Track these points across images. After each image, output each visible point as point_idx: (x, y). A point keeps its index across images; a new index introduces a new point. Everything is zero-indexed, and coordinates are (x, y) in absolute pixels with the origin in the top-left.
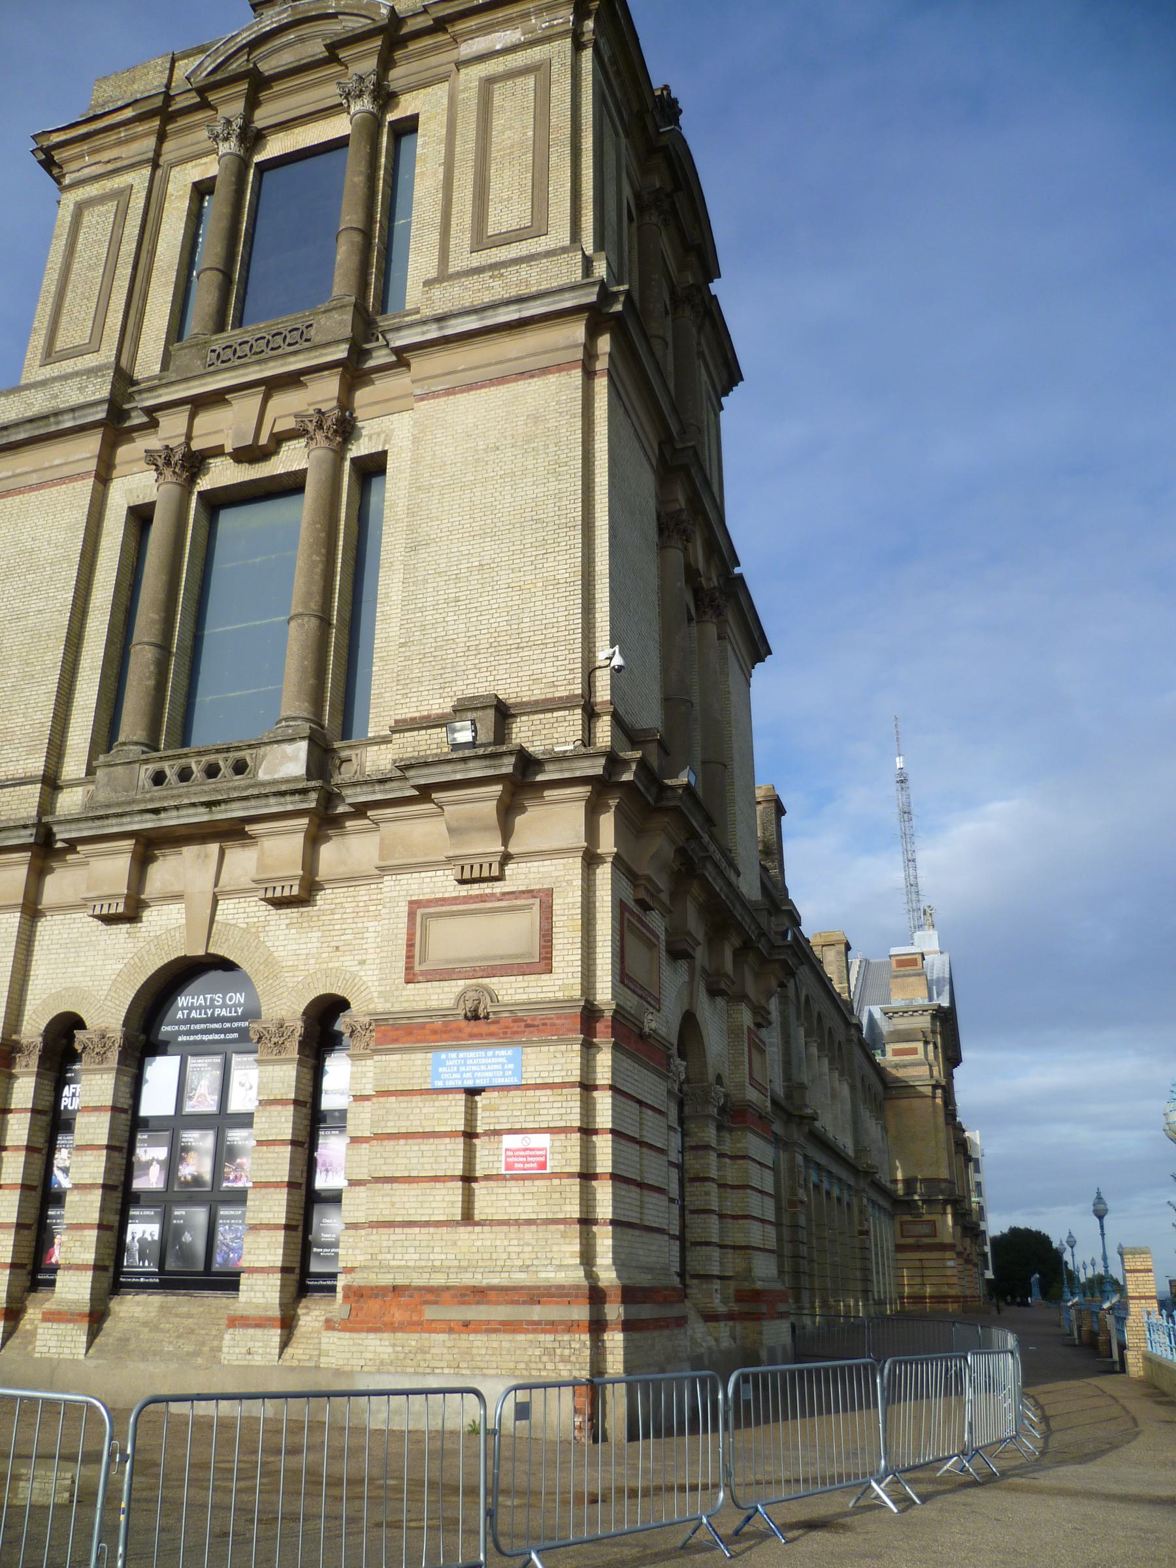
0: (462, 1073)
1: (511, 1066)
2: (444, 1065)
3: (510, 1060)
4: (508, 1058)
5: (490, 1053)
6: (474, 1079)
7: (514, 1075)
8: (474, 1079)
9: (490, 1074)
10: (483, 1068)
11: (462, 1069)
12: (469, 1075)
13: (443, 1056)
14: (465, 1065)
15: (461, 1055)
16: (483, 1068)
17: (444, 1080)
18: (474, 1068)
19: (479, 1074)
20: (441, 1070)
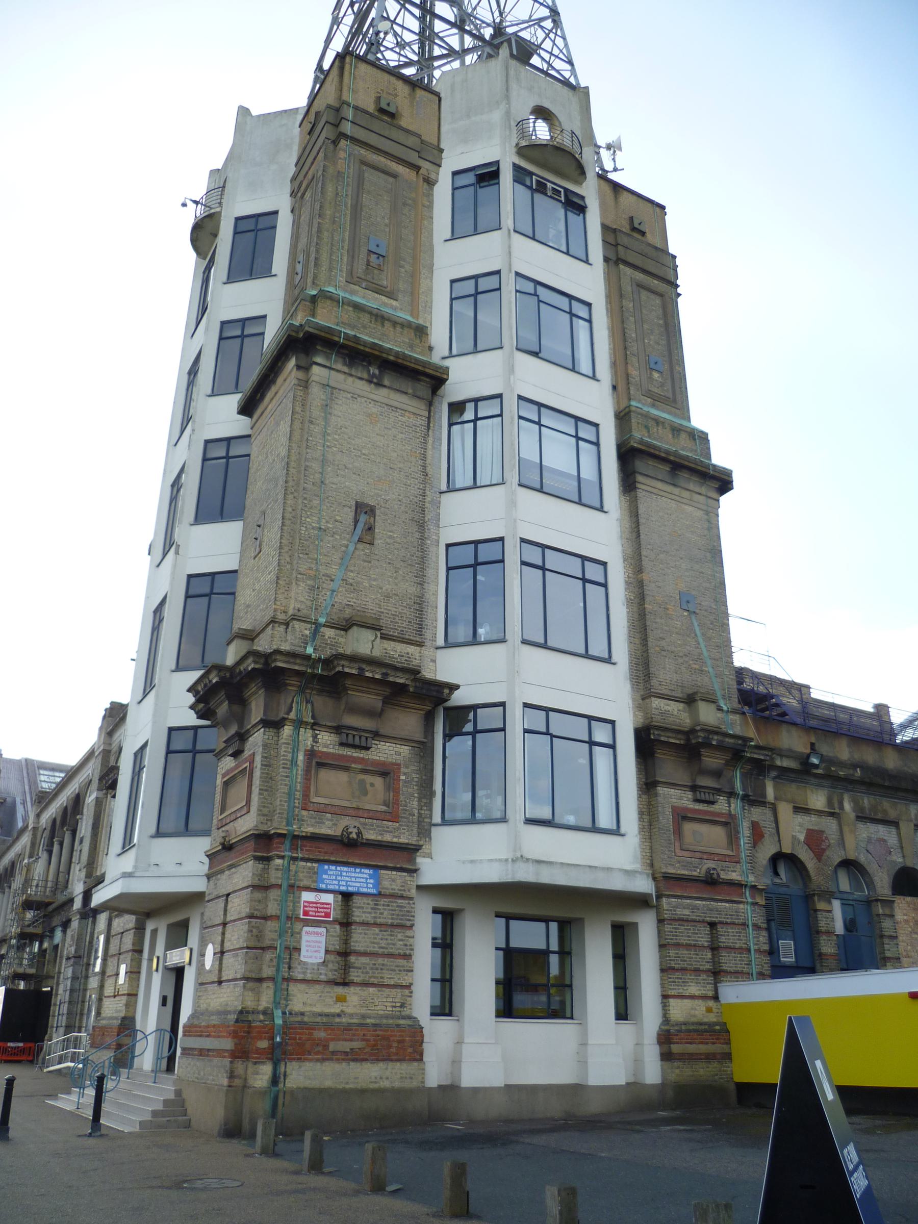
0: (339, 881)
1: (372, 881)
2: (326, 874)
3: (371, 877)
4: (370, 875)
5: (358, 870)
6: (347, 886)
7: (373, 888)
8: (347, 886)
9: (358, 885)
10: (353, 879)
11: (339, 878)
12: (344, 883)
13: (326, 867)
14: (341, 875)
15: (339, 868)
16: (353, 879)
17: (327, 885)
18: (347, 879)
19: (351, 884)
20: (324, 876)
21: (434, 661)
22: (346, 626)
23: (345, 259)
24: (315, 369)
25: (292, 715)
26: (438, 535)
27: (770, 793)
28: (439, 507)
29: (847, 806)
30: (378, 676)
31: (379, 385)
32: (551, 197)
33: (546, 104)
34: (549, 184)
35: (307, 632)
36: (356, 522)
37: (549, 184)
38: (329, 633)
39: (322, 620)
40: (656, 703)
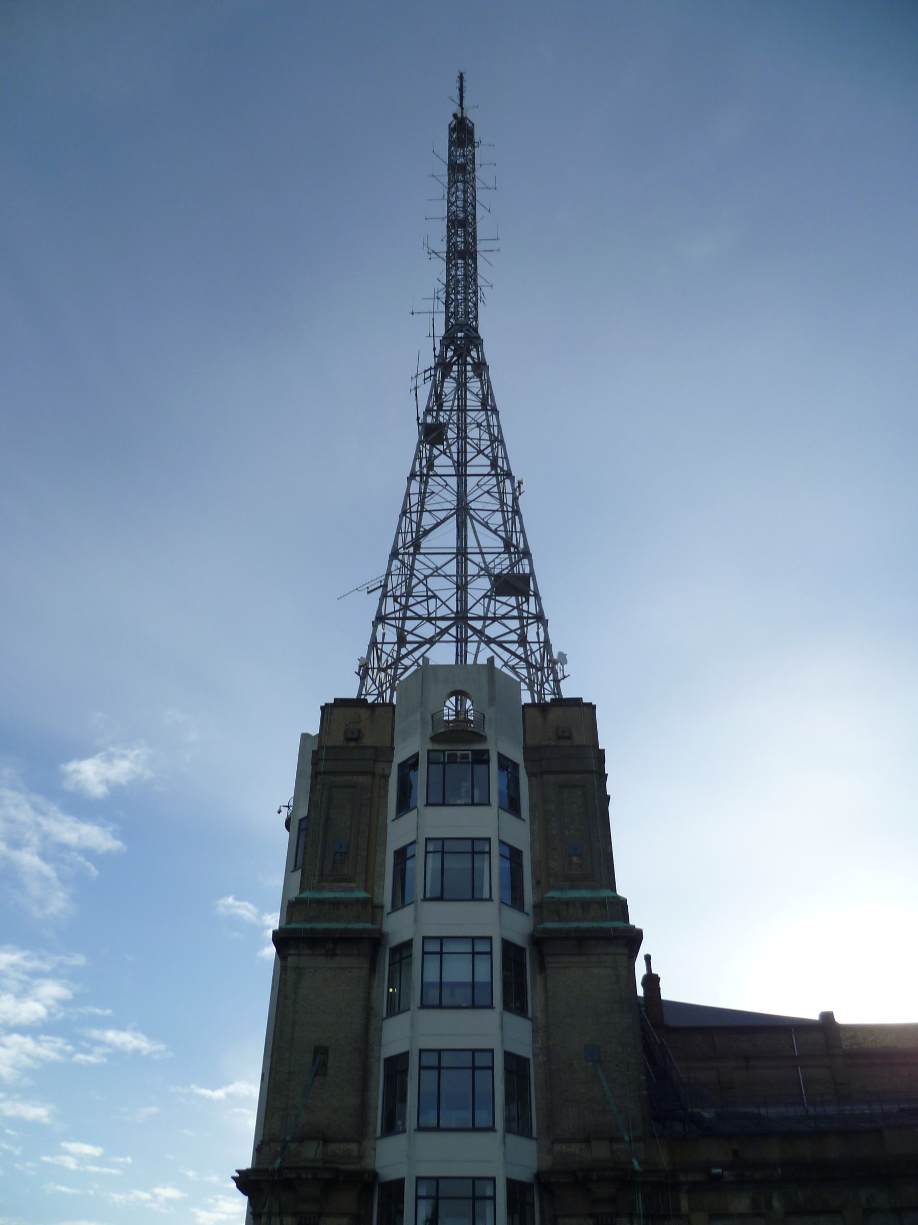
21: (374, 1149)
22: (300, 1139)
23: (318, 866)
24: (290, 959)
25: (266, 1209)
26: (380, 1052)
27: (684, 1205)
28: (381, 1031)
29: (776, 1204)
30: (310, 1176)
31: (334, 955)
32: (460, 763)
33: (459, 687)
34: (459, 753)
35: (279, 1149)
36: (314, 1060)
37: (459, 753)
38: (293, 1146)
39: (288, 1138)
40: (558, 1147)
